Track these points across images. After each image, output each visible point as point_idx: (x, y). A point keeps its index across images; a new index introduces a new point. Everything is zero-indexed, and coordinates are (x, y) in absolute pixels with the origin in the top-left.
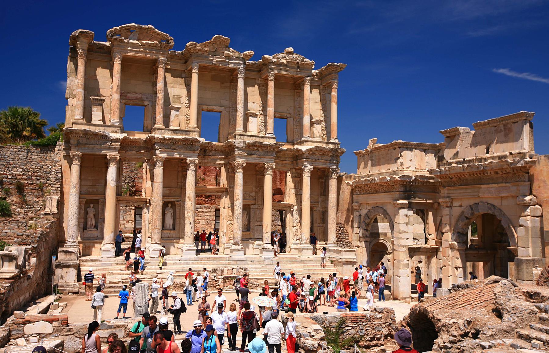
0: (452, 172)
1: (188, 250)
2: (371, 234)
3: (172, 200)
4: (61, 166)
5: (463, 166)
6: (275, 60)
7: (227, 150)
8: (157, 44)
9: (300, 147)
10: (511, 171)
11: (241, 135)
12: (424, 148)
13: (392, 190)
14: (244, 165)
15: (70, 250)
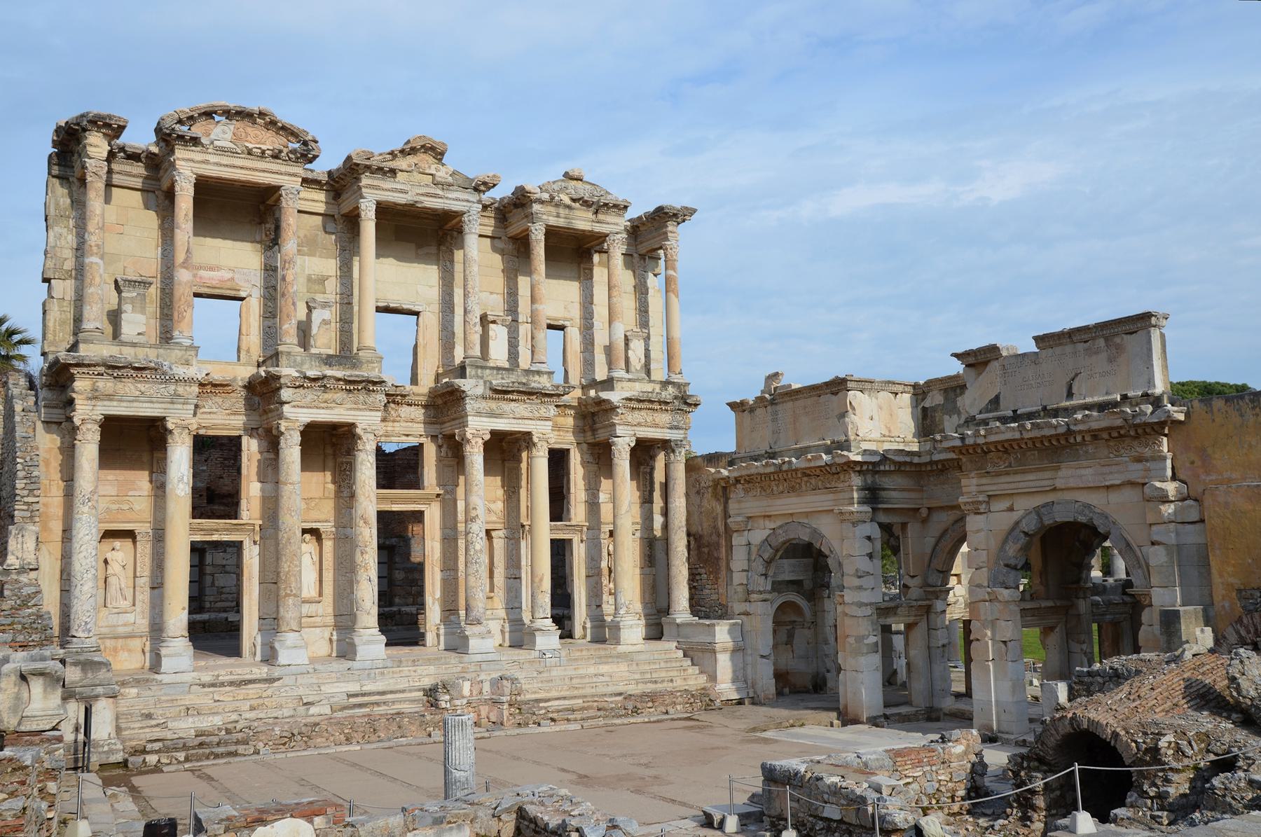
0: (992, 438)
1: (369, 642)
2: (773, 583)
3: (314, 525)
4: (37, 449)
5: (1023, 426)
6: (546, 196)
7: (440, 402)
8: (281, 151)
9: (604, 395)
10: (1132, 433)
11: (477, 367)
12: (895, 388)
13: (833, 484)
14: (487, 437)
15: (96, 659)
